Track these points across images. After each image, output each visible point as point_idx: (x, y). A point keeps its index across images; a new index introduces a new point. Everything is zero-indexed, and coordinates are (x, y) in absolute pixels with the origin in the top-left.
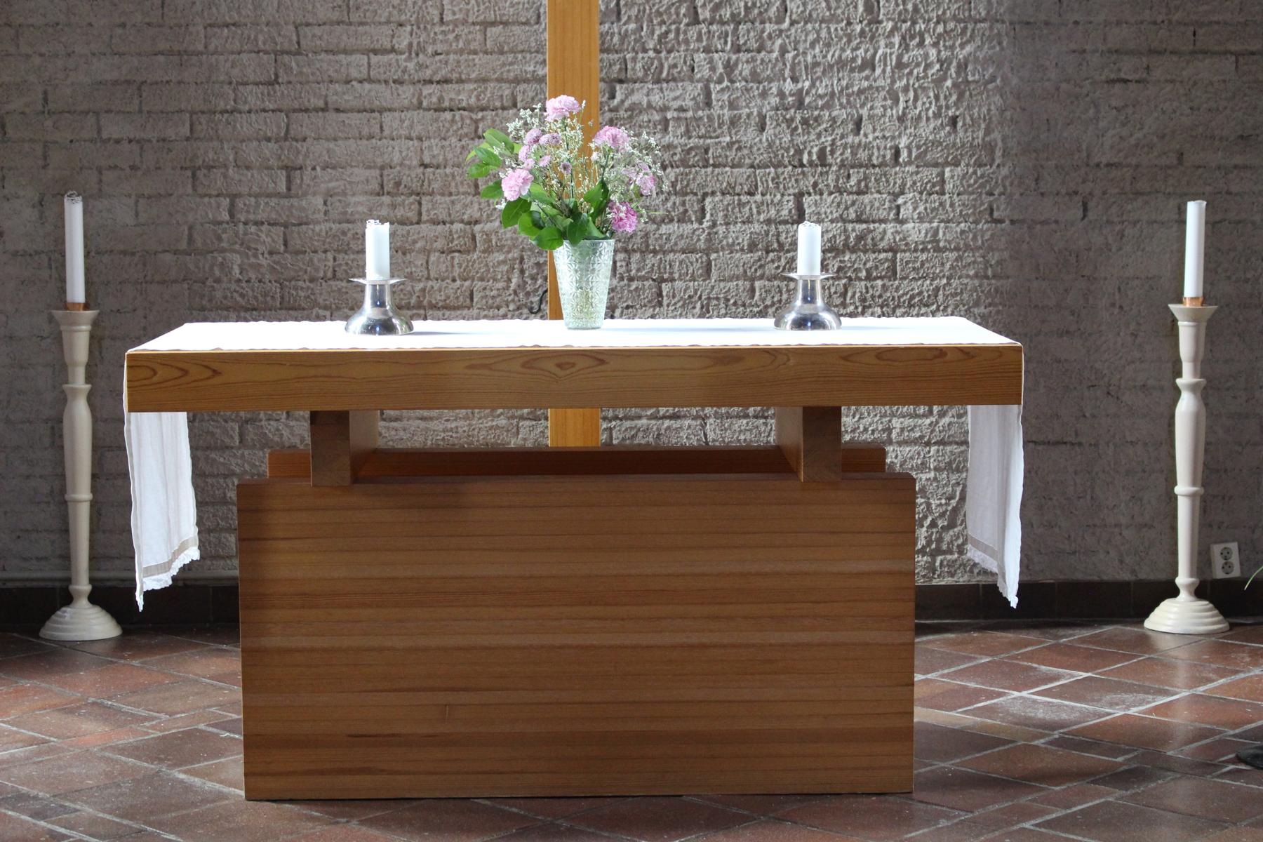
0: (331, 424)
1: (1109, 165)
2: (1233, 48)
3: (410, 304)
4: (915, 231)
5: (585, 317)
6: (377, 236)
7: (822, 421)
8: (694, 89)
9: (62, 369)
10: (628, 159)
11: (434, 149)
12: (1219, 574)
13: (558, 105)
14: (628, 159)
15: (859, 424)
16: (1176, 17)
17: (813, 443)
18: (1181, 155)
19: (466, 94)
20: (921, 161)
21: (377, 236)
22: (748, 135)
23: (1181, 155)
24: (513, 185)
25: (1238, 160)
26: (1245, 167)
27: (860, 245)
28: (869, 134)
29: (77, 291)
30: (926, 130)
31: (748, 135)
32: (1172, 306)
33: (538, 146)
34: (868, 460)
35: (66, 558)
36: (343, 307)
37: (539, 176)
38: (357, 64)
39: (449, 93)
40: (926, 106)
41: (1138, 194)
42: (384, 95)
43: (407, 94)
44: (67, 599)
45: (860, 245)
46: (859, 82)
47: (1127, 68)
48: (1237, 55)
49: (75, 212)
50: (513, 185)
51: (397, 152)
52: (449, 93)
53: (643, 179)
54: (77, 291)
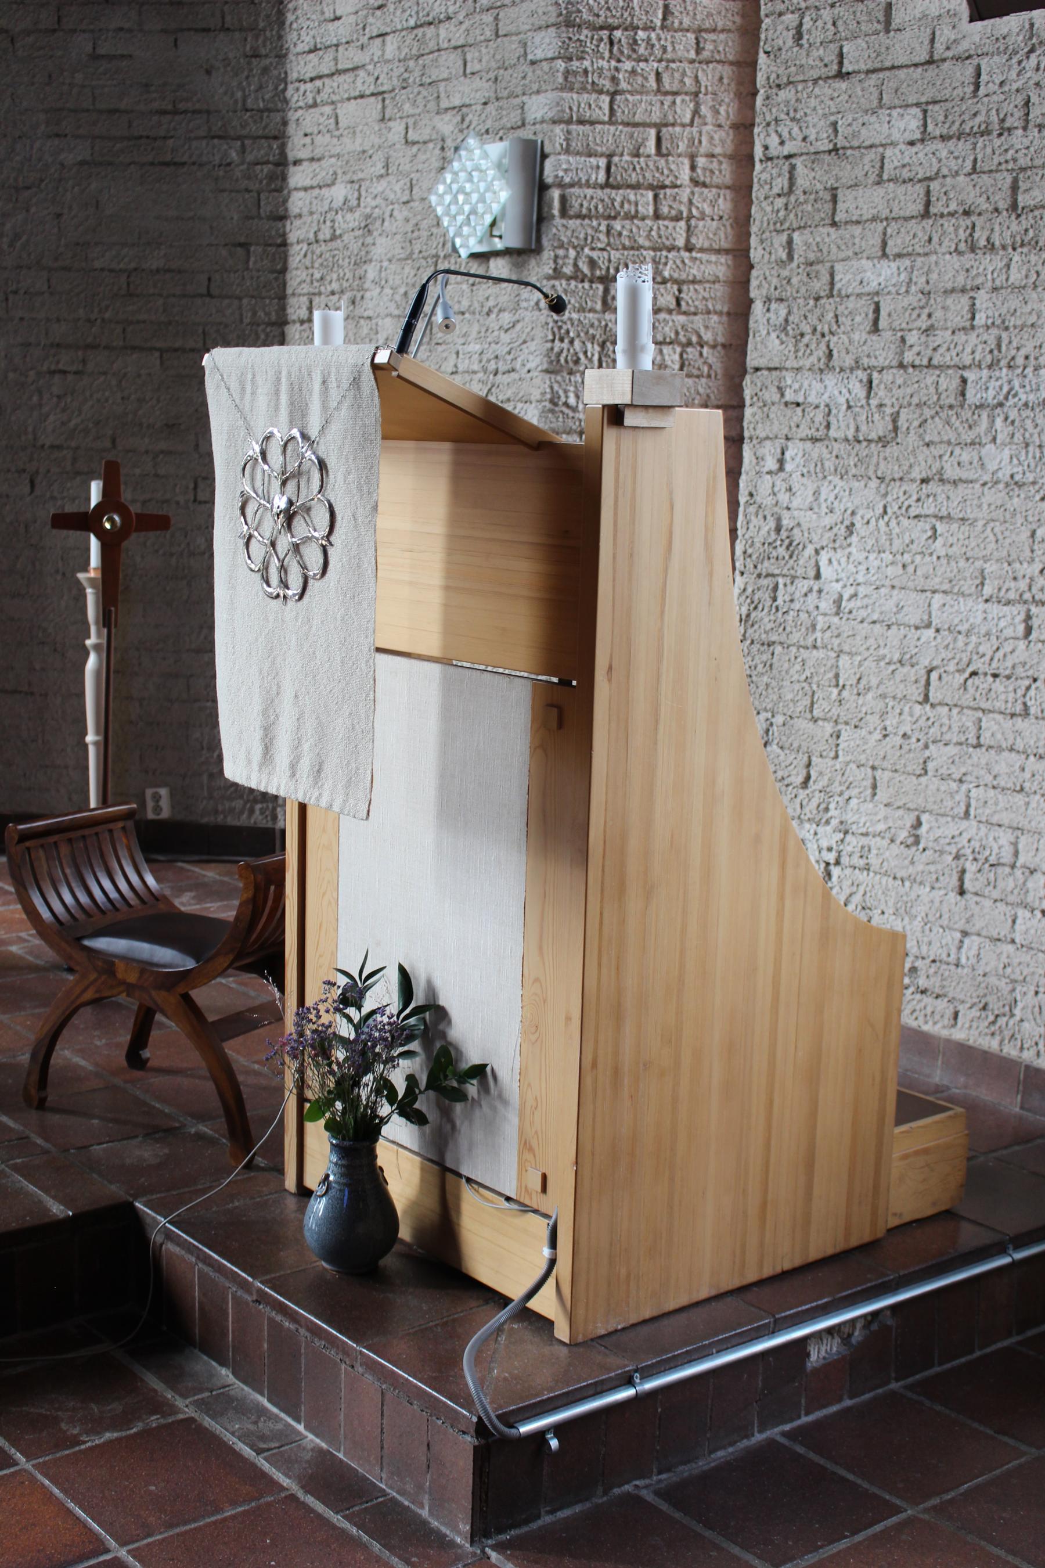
1: (52, 447)
2: (158, 345)
12: (151, 815)
16: (107, 315)
18: (113, 441)
23: (113, 441)
25: (163, 445)
26: (170, 453)
32: (81, 576)
41: (78, 473)
48: (162, 351)
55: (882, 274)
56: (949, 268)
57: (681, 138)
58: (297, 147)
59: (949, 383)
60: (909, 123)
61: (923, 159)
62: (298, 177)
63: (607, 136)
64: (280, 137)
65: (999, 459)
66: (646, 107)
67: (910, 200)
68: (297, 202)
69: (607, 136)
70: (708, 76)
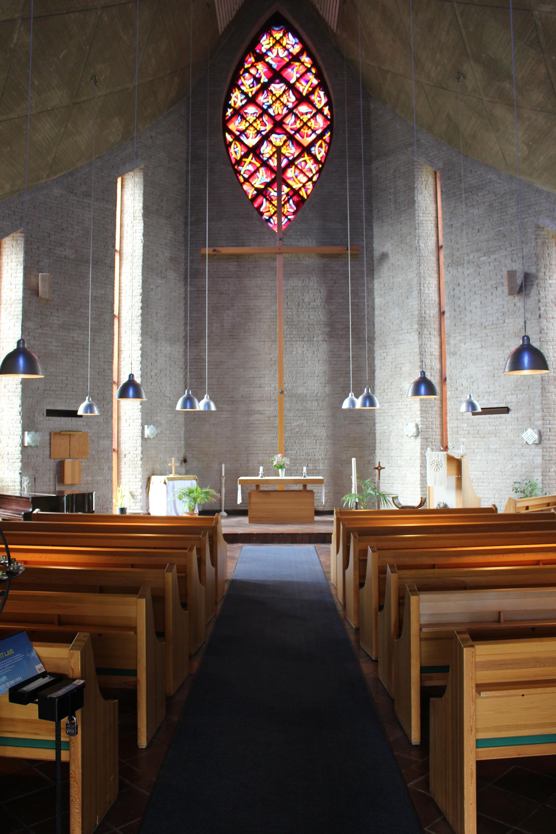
0: (258, 486)
3: (264, 475)
4: (322, 468)
5: (282, 476)
6: (261, 468)
7: (305, 486)
8: (295, 451)
9: (221, 484)
10: (286, 461)
11: (265, 458)
13: (279, 455)
14: (286, 461)
15: (309, 487)
17: (306, 490)
19: (268, 452)
20: (322, 460)
21: (261, 468)
22: (302, 457)
24: (275, 463)
27: (315, 469)
28: (316, 457)
29: (223, 474)
30: (323, 456)
31: (302, 457)
33: (278, 458)
34: (311, 492)
35: (221, 507)
36: (258, 475)
37: (278, 462)
38: (256, 448)
39: (267, 452)
40: (323, 453)
42: (259, 452)
43: (261, 452)
44: (221, 511)
45: (315, 469)
46: (315, 450)
47: (346, 449)
49: (223, 466)
50: (275, 463)
51: (260, 459)
52: (267, 452)
53: (288, 463)
54: (223, 474)
55: (464, 440)
56: (472, 439)
57: (434, 423)
58: (377, 421)
59: (472, 450)
60: (466, 425)
61: (468, 428)
62: (377, 425)
63: (426, 423)
64: (374, 420)
65: (479, 458)
66: (430, 420)
67: (467, 432)
68: (377, 428)
69: (426, 423)
70: (437, 416)
